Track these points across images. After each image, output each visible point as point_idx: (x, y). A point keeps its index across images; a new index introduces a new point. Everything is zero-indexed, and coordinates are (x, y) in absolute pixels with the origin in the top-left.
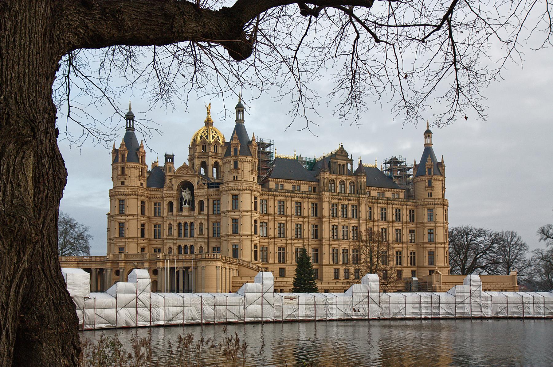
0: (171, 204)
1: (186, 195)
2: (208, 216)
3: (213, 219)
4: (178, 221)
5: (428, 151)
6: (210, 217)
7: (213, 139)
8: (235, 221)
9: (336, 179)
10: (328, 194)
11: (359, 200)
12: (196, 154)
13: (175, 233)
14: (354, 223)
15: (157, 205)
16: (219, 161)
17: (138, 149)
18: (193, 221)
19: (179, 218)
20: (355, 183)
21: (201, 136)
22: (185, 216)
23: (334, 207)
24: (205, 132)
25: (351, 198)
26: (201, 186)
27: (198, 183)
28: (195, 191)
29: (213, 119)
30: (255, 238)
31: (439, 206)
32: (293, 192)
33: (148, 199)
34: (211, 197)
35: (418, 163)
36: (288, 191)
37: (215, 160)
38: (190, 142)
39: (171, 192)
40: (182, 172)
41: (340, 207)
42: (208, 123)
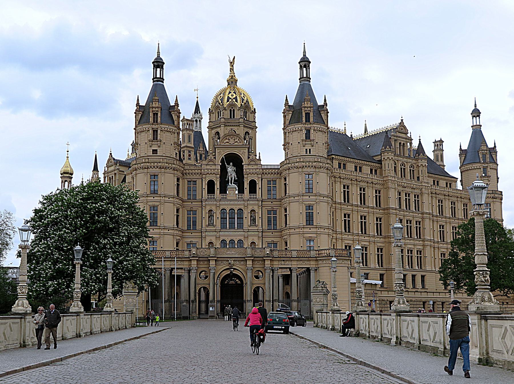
0: (211, 185)
2: (262, 201)
4: (222, 207)
6: (263, 203)
8: (309, 207)
16: (250, 131)
18: (242, 207)
19: (223, 203)
20: (415, 168)
22: (231, 200)
24: (232, 93)
26: (252, 161)
27: (249, 158)
29: (237, 77)
31: (497, 200)
34: (266, 175)
39: (213, 167)
40: (227, 141)
42: (232, 81)
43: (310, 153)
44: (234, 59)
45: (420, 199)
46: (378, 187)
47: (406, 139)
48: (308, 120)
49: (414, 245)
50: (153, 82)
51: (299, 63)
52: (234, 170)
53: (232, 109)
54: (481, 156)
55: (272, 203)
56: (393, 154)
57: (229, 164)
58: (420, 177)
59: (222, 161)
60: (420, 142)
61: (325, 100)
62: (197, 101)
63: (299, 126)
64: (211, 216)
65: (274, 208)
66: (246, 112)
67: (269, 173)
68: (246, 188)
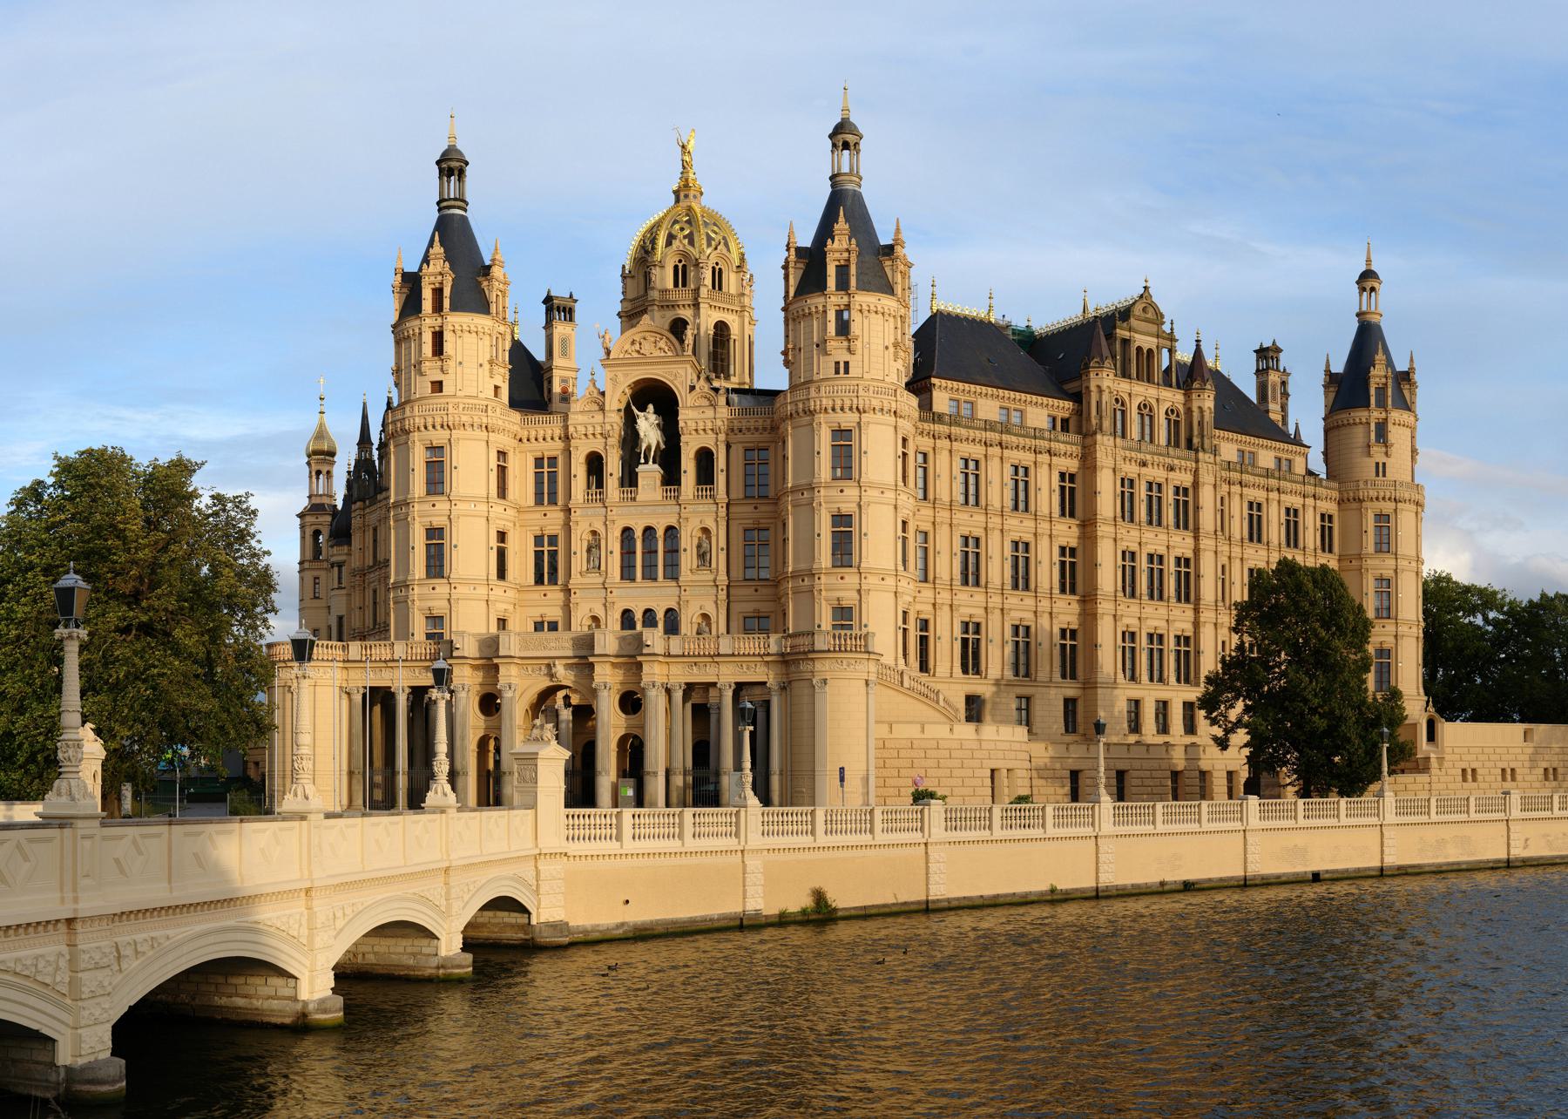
0: (595, 464)
1: (649, 429)
2: (728, 505)
6: (732, 509)
7: (709, 245)
10: (1111, 442)
11: (1197, 470)
12: (654, 295)
13: (614, 564)
14: (1181, 544)
17: (486, 270)
18: (673, 521)
21: (671, 238)
22: (646, 505)
25: (1176, 462)
27: (692, 388)
32: (1005, 428)
34: (740, 436)
36: (989, 426)
37: (717, 316)
38: (625, 254)
39: (599, 417)
40: (637, 347)
43: (847, 371)
45: (1190, 499)
48: (843, 285)
49: (1172, 619)
51: (831, 136)
52: (658, 425)
53: (680, 265)
55: (756, 508)
56: (1111, 376)
57: (643, 409)
58: (1196, 440)
61: (898, 231)
63: (815, 301)
64: (593, 547)
65: (761, 521)
66: (720, 269)
67: (749, 429)
68: (685, 472)
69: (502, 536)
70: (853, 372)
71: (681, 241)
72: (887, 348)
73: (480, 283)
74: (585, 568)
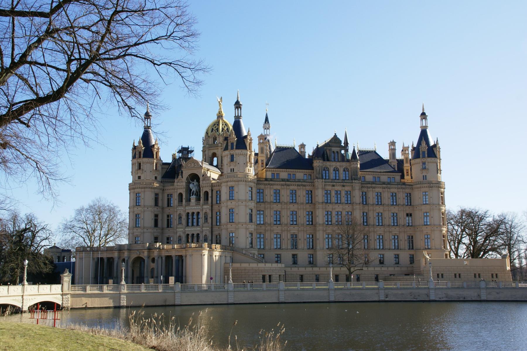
0: (181, 195)
3: (216, 207)
4: (187, 211)
5: (424, 135)
9: (330, 166)
13: (184, 221)
14: (348, 208)
15: (170, 197)
18: (199, 211)
23: (327, 194)
28: (201, 182)
30: (250, 226)
33: (161, 191)
35: (415, 146)
36: (283, 180)
39: (181, 184)
40: (190, 165)
41: (333, 193)
43: (233, 171)
44: (221, 99)
46: (308, 188)
47: (339, 147)
50: (144, 129)
51: (234, 105)
54: (421, 153)
59: (187, 179)
60: (354, 148)
62: (267, 114)
64: (180, 218)
69: (156, 216)
70: (235, 171)
71: (215, 131)
72: (244, 164)
73: (152, 149)
74: (178, 223)
